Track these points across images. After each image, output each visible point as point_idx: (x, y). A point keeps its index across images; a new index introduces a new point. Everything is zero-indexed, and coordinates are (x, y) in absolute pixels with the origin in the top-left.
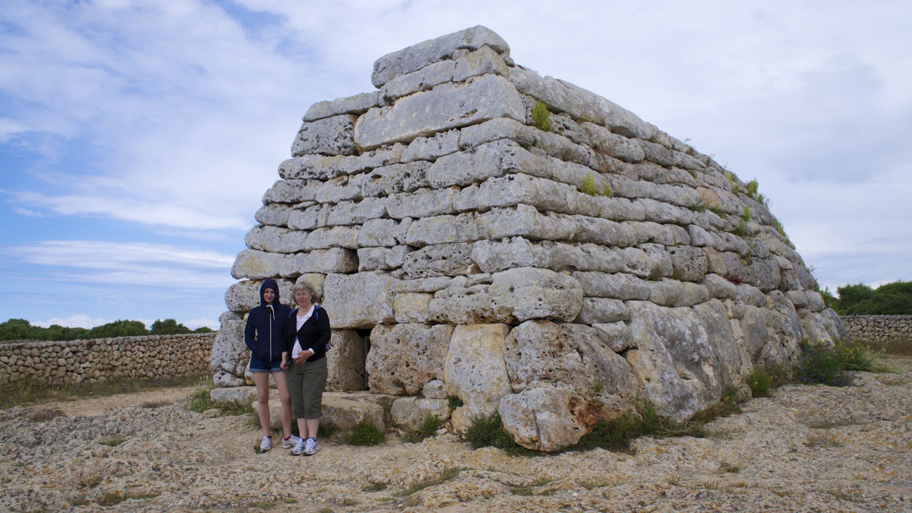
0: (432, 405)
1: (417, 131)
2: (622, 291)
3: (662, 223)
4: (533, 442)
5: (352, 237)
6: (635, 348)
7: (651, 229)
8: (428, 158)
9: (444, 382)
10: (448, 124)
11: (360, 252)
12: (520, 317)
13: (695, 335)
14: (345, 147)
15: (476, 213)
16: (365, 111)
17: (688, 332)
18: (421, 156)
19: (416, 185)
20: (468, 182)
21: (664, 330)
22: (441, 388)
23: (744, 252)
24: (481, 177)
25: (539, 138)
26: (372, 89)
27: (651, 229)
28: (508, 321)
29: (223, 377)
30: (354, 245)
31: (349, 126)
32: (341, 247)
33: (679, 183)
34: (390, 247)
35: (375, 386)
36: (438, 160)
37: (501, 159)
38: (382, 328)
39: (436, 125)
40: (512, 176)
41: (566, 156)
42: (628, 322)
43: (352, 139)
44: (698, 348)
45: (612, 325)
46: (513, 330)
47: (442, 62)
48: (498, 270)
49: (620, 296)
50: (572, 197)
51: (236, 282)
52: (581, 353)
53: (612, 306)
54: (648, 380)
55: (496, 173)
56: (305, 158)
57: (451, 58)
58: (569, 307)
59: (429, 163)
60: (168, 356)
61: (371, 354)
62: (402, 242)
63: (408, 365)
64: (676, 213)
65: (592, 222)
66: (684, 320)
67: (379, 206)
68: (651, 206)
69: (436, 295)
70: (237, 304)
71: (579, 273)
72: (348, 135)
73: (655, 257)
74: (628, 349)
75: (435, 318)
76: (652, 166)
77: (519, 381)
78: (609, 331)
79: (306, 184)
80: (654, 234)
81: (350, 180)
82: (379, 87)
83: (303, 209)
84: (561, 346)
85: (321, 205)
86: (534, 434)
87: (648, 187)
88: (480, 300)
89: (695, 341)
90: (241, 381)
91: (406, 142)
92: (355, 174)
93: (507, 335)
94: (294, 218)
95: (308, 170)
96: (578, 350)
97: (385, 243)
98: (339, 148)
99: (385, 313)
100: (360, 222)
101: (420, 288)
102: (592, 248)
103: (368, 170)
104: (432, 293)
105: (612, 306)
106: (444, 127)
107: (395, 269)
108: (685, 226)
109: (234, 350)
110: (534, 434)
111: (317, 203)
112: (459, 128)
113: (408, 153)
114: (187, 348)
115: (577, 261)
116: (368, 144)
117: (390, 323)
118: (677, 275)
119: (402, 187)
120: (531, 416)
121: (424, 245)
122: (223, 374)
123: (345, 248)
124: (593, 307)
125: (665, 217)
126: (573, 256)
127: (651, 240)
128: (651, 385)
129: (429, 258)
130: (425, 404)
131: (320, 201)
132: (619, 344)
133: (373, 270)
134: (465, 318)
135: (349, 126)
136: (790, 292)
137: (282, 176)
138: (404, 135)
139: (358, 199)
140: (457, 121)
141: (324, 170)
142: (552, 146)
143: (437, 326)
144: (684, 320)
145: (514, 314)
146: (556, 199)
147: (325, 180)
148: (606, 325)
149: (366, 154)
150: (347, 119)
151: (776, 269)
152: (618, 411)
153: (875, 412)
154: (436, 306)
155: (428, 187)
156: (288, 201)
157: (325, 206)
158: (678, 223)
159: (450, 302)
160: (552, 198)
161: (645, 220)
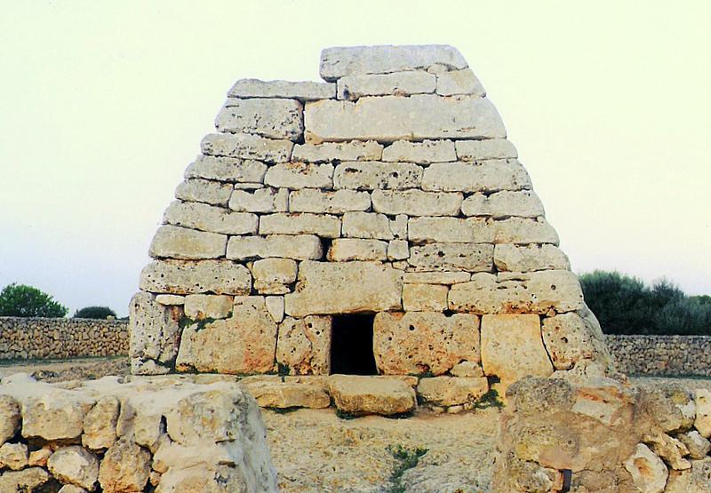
5: (328, 227)
8: (418, 162)
14: (292, 133)
15: (491, 219)
47: (416, 72)
55: (509, 188)
62: (401, 236)
75: (456, 308)
77: (563, 360)
83: (251, 191)
85: (276, 190)
88: (514, 294)
94: (238, 199)
99: (394, 301)
103: (336, 163)
104: (449, 286)
106: (436, 136)
109: (162, 335)
112: (454, 140)
113: (391, 154)
117: (399, 310)
119: (387, 185)
130: (461, 382)
150: (294, 104)
154: (457, 298)
157: (283, 192)
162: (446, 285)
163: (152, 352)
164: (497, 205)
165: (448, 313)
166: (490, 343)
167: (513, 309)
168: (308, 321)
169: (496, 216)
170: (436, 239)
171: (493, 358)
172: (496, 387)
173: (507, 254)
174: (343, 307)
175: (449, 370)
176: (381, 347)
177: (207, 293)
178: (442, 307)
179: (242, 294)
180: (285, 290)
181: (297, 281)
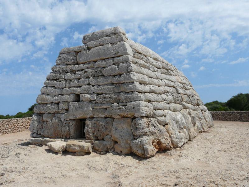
0: (108, 144)
1: (99, 58)
3: (169, 87)
4: (143, 155)
6: (167, 124)
7: (167, 88)
8: (103, 66)
9: (111, 136)
10: (110, 57)
11: (81, 95)
12: (136, 117)
13: (182, 120)
14: (74, 62)
15: (120, 84)
16: (80, 51)
17: (180, 119)
18: (101, 66)
19: (99, 75)
20: (117, 74)
21: (174, 119)
22: (110, 138)
23: (189, 95)
24: (121, 73)
26: (83, 45)
27: (167, 88)
28: (132, 117)
29: (33, 135)
30: (79, 93)
31: (75, 56)
32: (74, 93)
33: (171, 75)
34: (91, 94)
35: (88, 137)
37: (128, 68)
39: (105, 57)
40: (131, 73)
41: (144, 66)
42: (165, 116)
43: (76, 60)
44: (183, 124)
46: (134, 120)
48: (128, 102)
49: (162, 109)
50: (147, 79)
52: (155, 127)
53: (160, 112)
54: (172, 134)
55: (126, 72)
57: (109, 36)
58: (150, 113)
59: (103, 68)
60: (5, 126)
61: (86, 127)
62: (95, 92)
63: (99, 131)
64: (172, 84)
65: (153, 87)
66: (179, 116)
67: (87, 81)
68: (167, 82)
69: (107, 109)
71: (152, 102)
72: (75, 59)
73: (170, 97)
74: (165, 125)
75: (107, 116)
76: (164, 70)
78: (160, 119)
79: (61, 74)
80: (168, 90)
81: (76, 72)
82: (85, 44)
84: (149, 125)
85: (67, 80)
86: (143, 152)
87: (165, 76)
89: (182, 122)
90: (40, 135)
91: (95, 62)
92: (78, 71)
93: (132, 121)
95: (62, 69)
96: (154, 126)
97: (89, 93)
98: (72, 63)
100: (80, 86)
101: (102, 107)
102: (154, 95)
103: (83, 70)
104: (106, 108)
105: (160, 112)
106: (108, 57)
107: (93, 101)
108: (175, 87)
110: (143, 152)
111: (65, 80)
112: (113, 58)
114: (12, 123)
115: (151, 99)
116: (82, 62)
117: (92, 118)
118: (175, 102)
119: (94, 75)
120: (142, 146)
121: (102, 94)
122: (33, 134)
123: (76, 94)
124: (156, 113)
125: (170, 85)
126: (150, 97)
127: (167, 92)
128: (172, 135)
129: (105, 98)
130: (105, 143)
131: (67, 79)
132: (163, 124)
133: (86, 101)
135: (75, 56)
136: (199, 106)
137: (53, 70)
138: (95, 59)
141: (67, 69)
142: (141, 64)
143: (108, 118)
144: (179, 116)
145: (134, 115)
146: (144, 80)
147: (68, 72)
148: (160, 118)
149: (82, 65)
151: (196, 100)
152: (165, 144)
153: (230, 141)
155: (103, 76)
156: (55, 78)
157: (68, 81)
158: (173, 87)
161: (165, 86)
162: (105, 108)
163: (35, 131)
164: (122, 79)
165: (106, 118)
166: (114, 129)
167: (123, 117)
168: (69, 122)
169: (121, 83)
170: (104, 92)
171: (116, 135)
172: (116, 146)
173: (123, 96)
174: (79, 117)
175: (103, 138)
177: (48, 113)
178: (103, 116)
180: (65, 111)
181: (68, 109)
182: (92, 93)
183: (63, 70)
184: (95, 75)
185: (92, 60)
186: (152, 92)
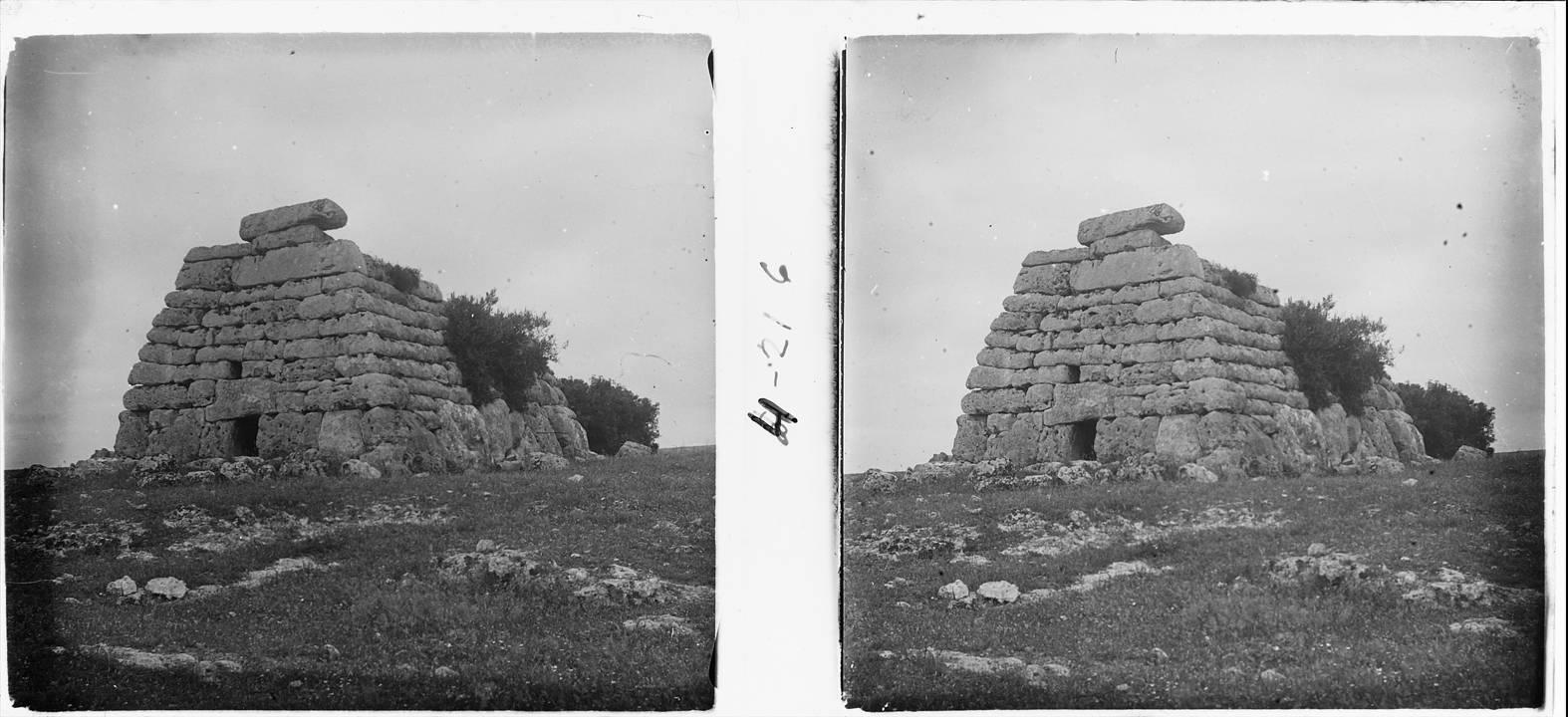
2: (1269, 396)
10: (1153, 278)
11: (1082, 368)
12: (1209, 409)
25: (1214, 292)
30: (1077, 363)
34: (1108, 365)
36: (1143, 304)
38: (1105, 421)
45: (1263, 417)
48: (1192, 380)
50: (1235, 333)
51: (970, 391)
53: (1263, 405)
56: (1027, 296)
70: (973, 408)
96: (1244, 430)
105: (1263, 405)
121: (1134, 363)
134: (1170, 411)
137: (1006, 309)
139: (1078, 329)
140: (1157, 277)
159: (1158, 401)
160: (1225, 333)
176: (1101, 444)
179: (1024, 412)
182: (1110, 362)
183: (1033, 308)
184: (1118, 322)
185: (1109, 285)
186: (1250, 362)
